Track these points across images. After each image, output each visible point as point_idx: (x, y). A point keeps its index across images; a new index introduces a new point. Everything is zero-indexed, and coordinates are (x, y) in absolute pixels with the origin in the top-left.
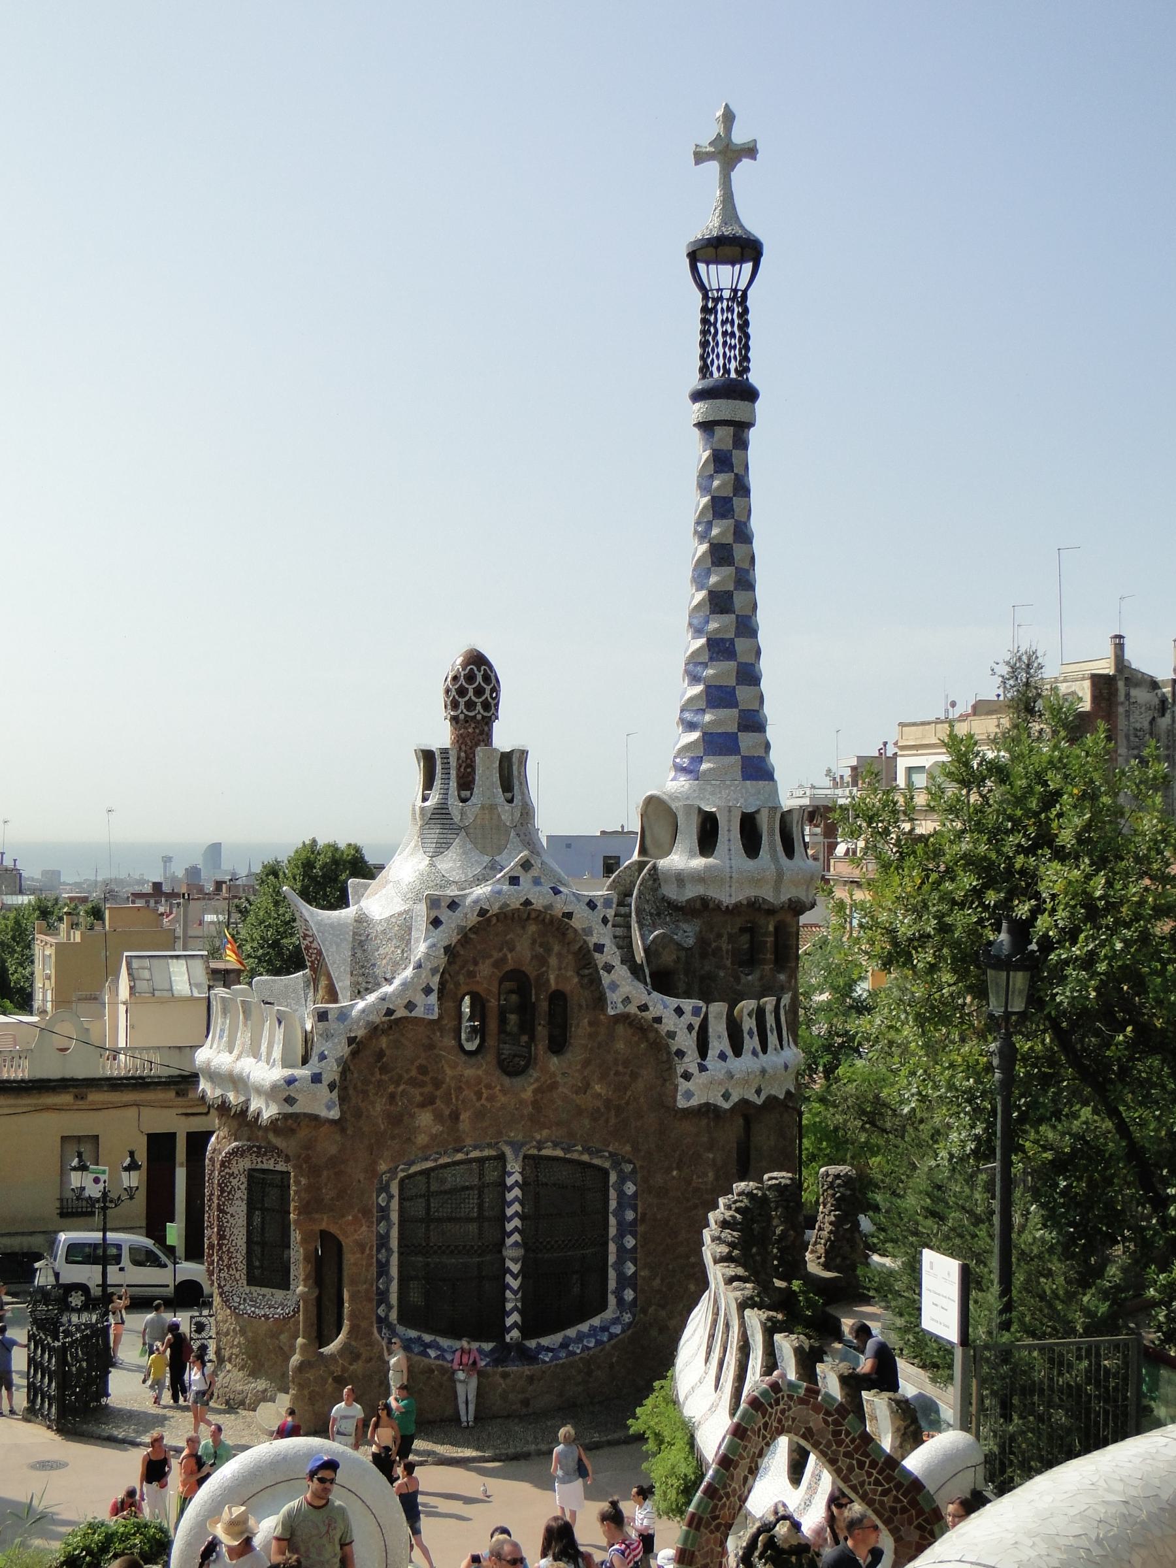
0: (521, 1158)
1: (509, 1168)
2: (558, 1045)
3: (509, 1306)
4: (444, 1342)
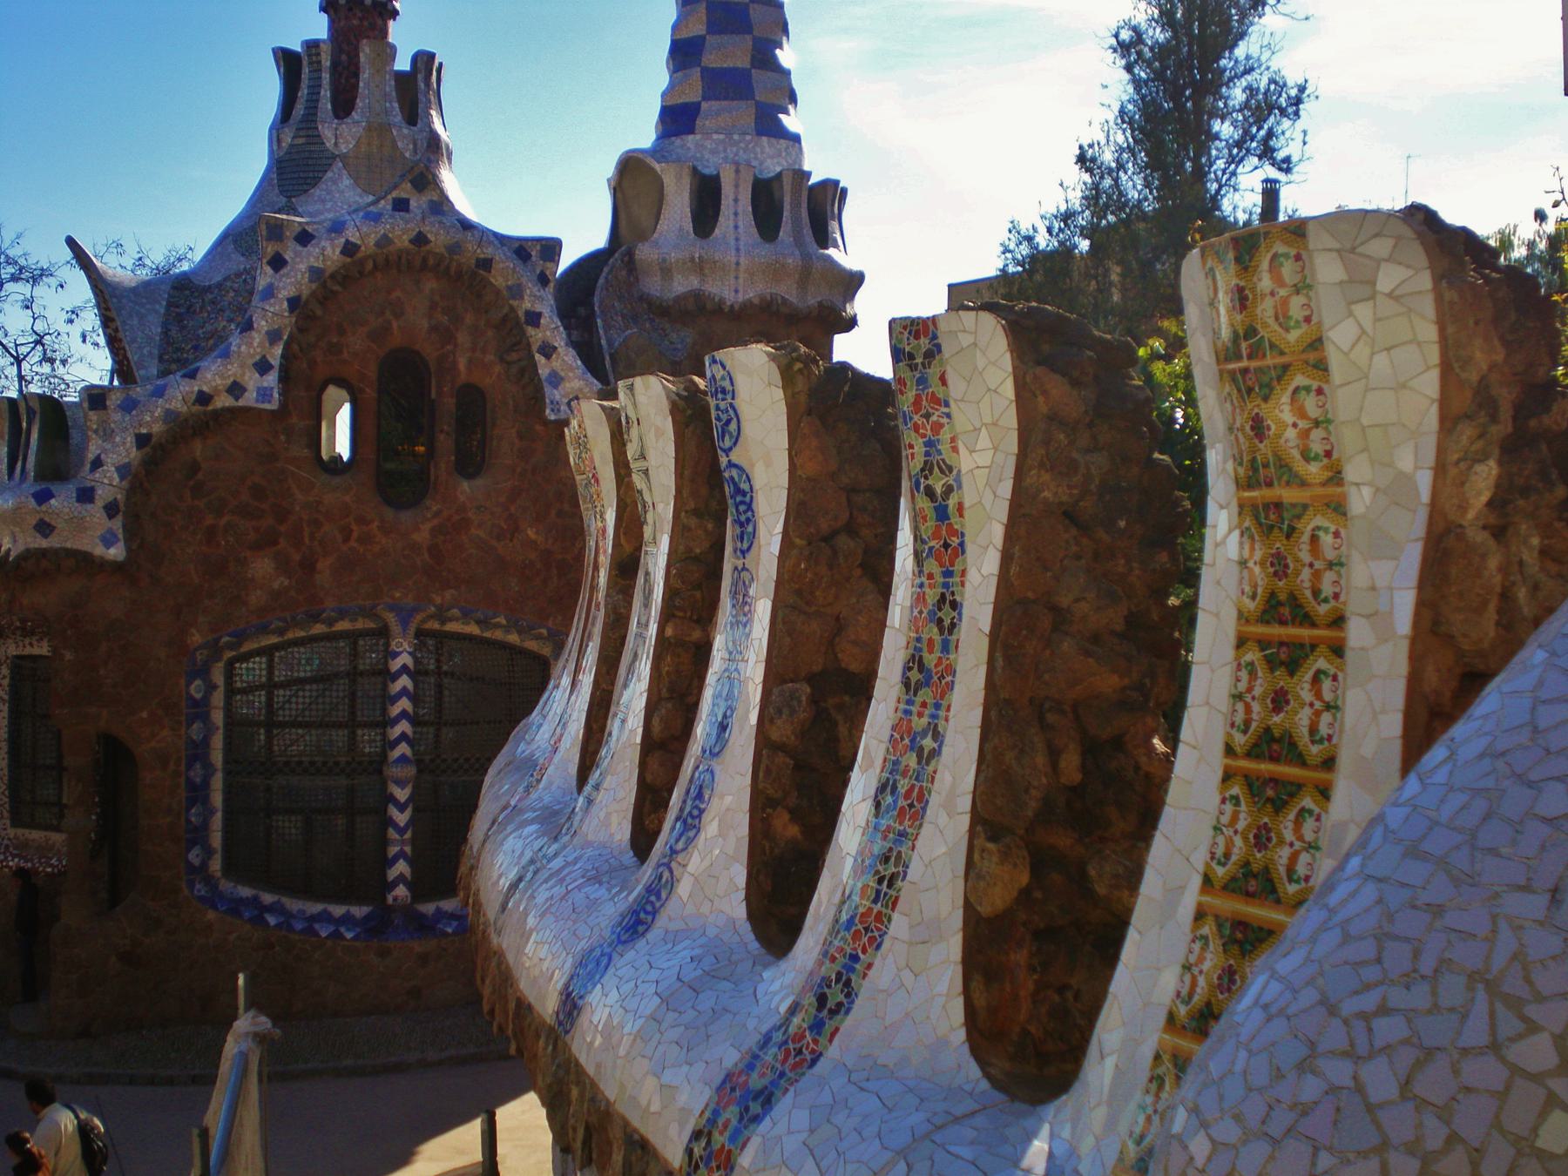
0: (412, 630)
1: (393, 646)
2: (470, 463)
3: (393, 850)
4: (293, 905)
